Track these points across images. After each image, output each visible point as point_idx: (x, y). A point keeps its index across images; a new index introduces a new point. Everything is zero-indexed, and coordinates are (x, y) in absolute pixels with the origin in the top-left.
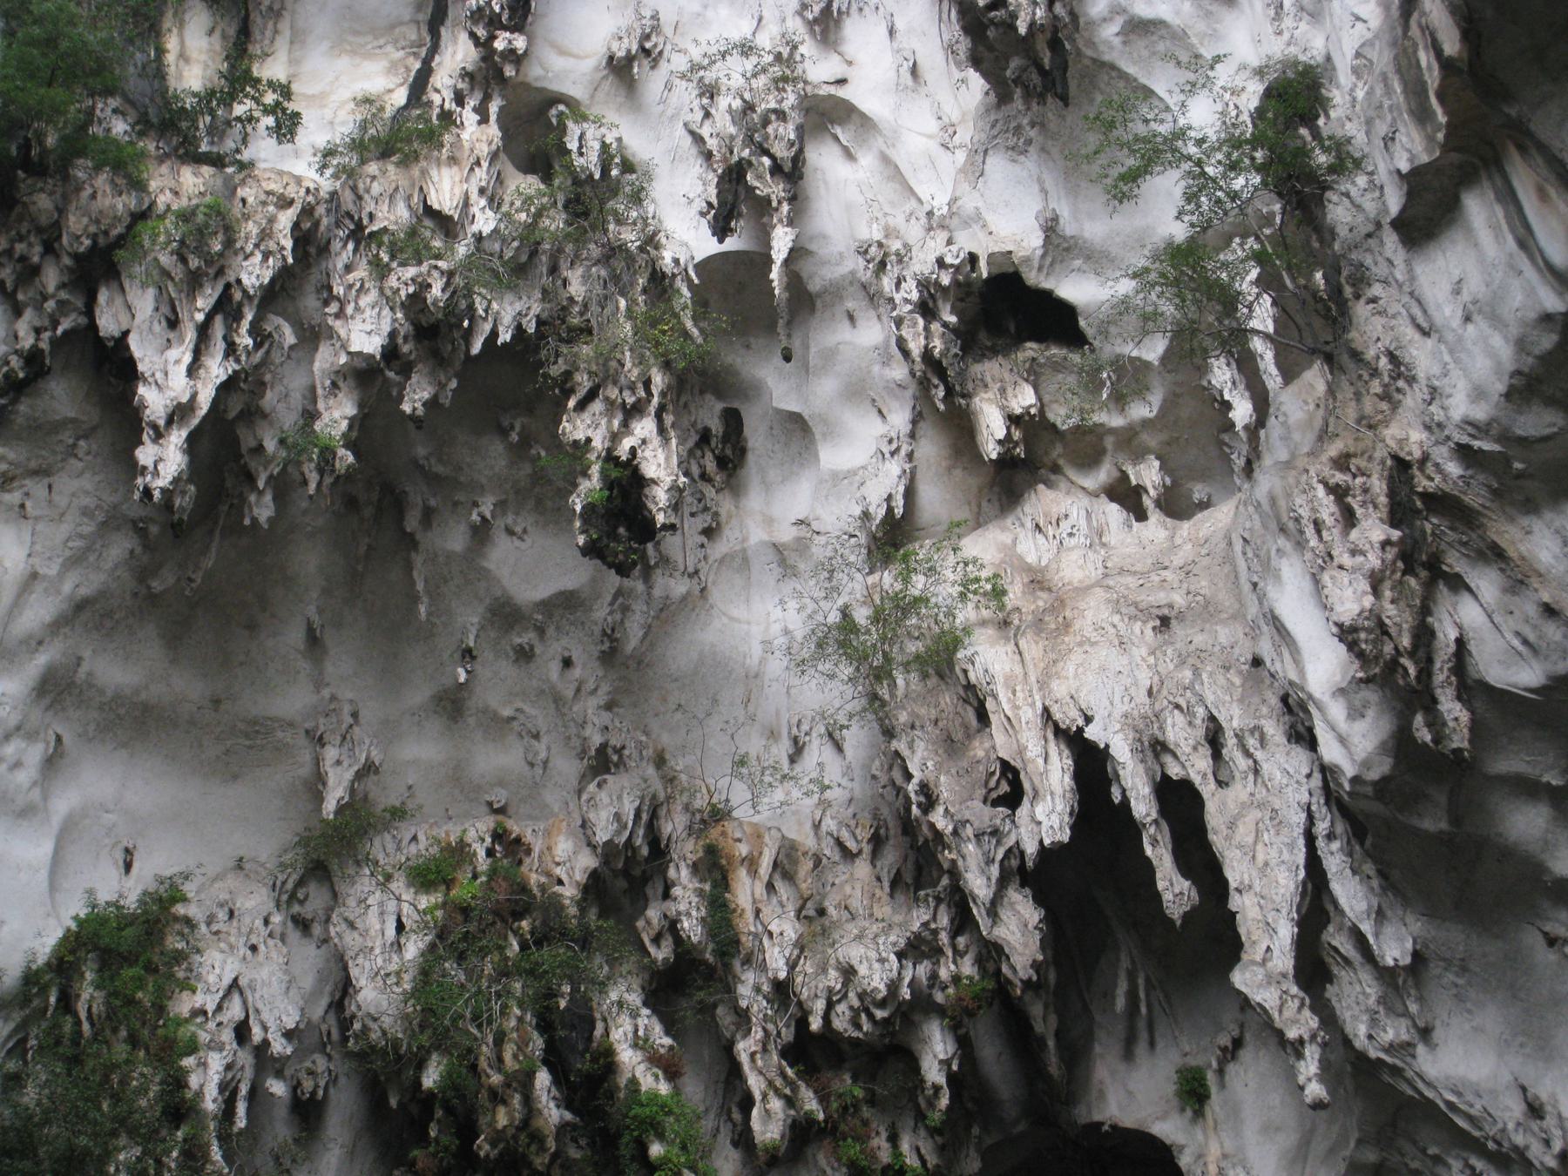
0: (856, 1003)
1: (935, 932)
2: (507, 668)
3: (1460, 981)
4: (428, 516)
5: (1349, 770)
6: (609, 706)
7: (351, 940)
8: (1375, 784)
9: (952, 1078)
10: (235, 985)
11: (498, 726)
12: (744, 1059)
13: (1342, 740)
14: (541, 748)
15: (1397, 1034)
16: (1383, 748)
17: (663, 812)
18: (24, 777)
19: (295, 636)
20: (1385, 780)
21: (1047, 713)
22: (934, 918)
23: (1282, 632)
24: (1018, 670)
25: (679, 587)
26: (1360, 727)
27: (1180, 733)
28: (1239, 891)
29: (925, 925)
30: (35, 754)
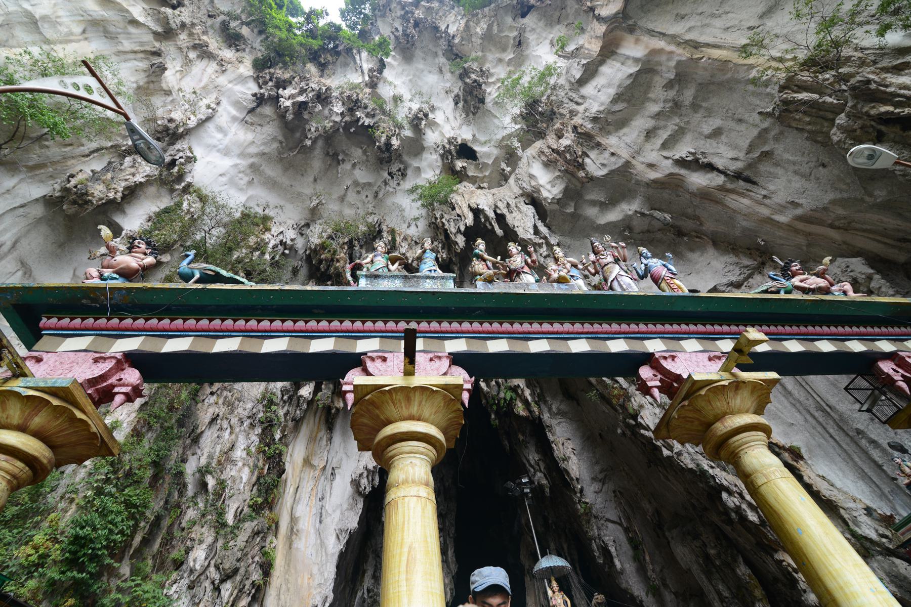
2: (354, 195)
4: (343, 160)
5: (551, 197)
7: (311, 234)
10: (282, 232)
11: (351, 205)
13: (549, 191)
14: (359, 211)
18: (242, 182)
19: (311, 179)
21: (469, 206)
23: (531, 176)
25: (391, 190)
27: (500, 204)
30: (246, 179)
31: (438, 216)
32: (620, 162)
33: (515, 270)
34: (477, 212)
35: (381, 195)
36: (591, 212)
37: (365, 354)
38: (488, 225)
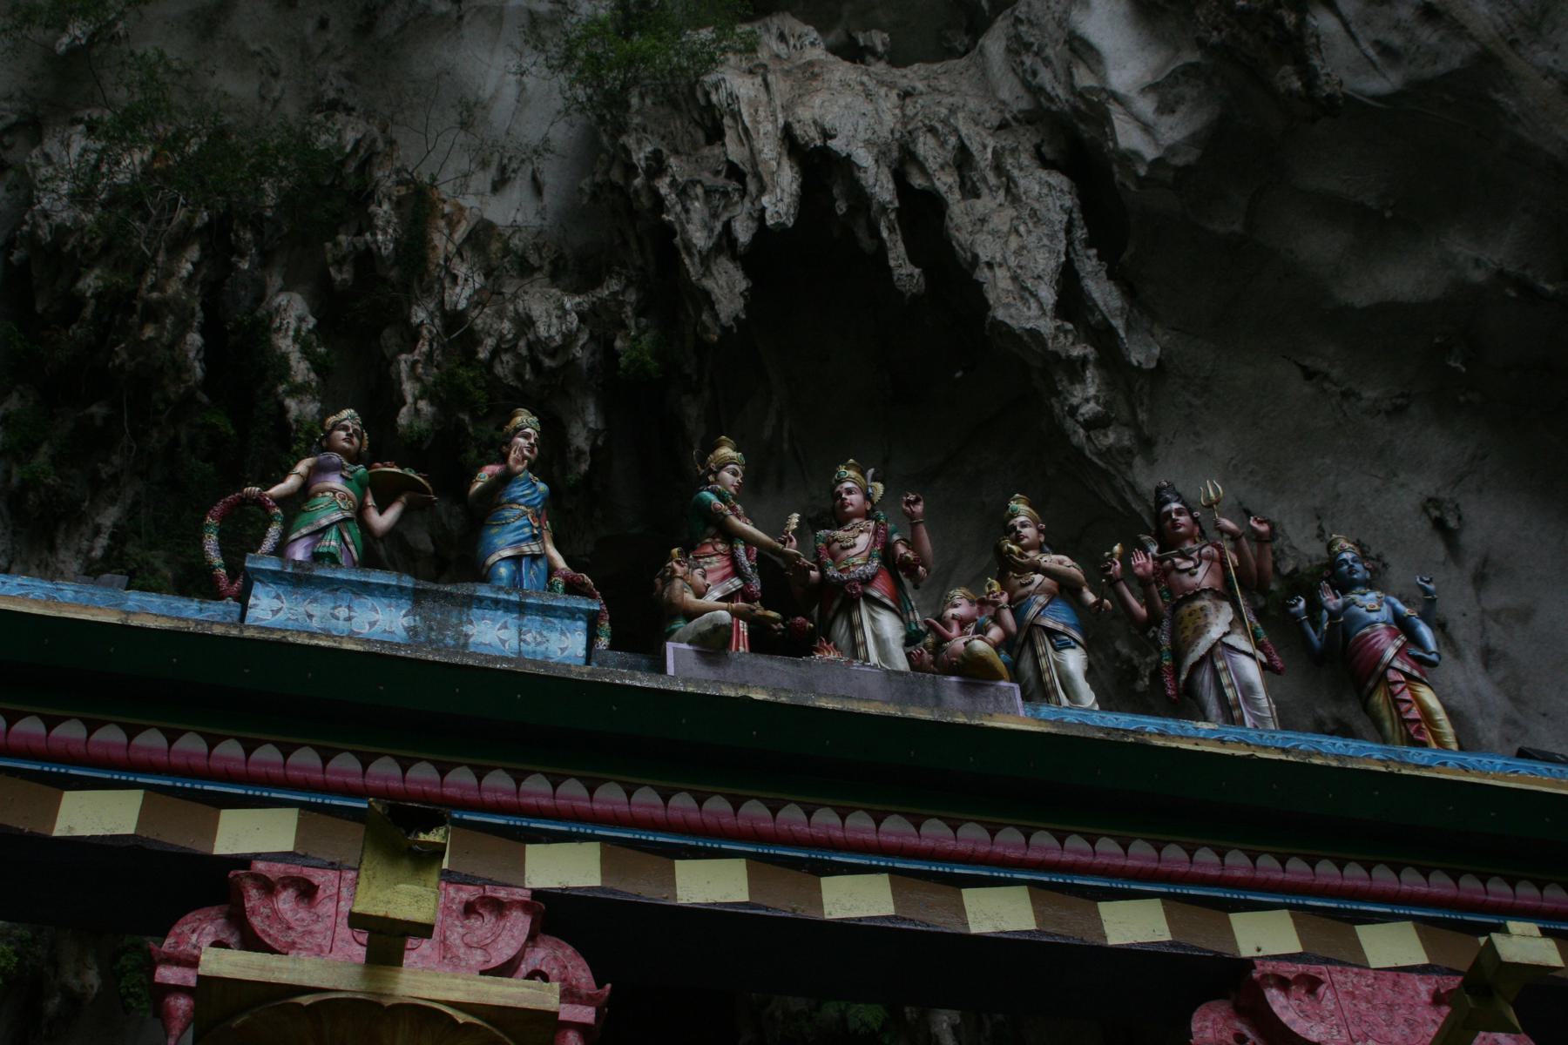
0: (524, 351)
1: (622, 304)
3: (1197, 402)
5: (1150, 153)
6: (349, 76)
8: (1177, 169)
9: (594, 450)
12: (404, 367)
13: (1147, 128)
14: (277, 87)
15: (1119, 439)
16: (1193, 139)
17: (376, 160)
20: (1187, 168)
22: (623, 293)
24: (763, 97)
26: (1167, 120)
28: (990, 265)
29: (614, 294)
31: (640, 157)
32: (1456, 55)
33: (840, 585)
34: (819, 165)
35: (388, 26)
36: (1318, 246)
37: (243, 861)
38: (862, 234)
